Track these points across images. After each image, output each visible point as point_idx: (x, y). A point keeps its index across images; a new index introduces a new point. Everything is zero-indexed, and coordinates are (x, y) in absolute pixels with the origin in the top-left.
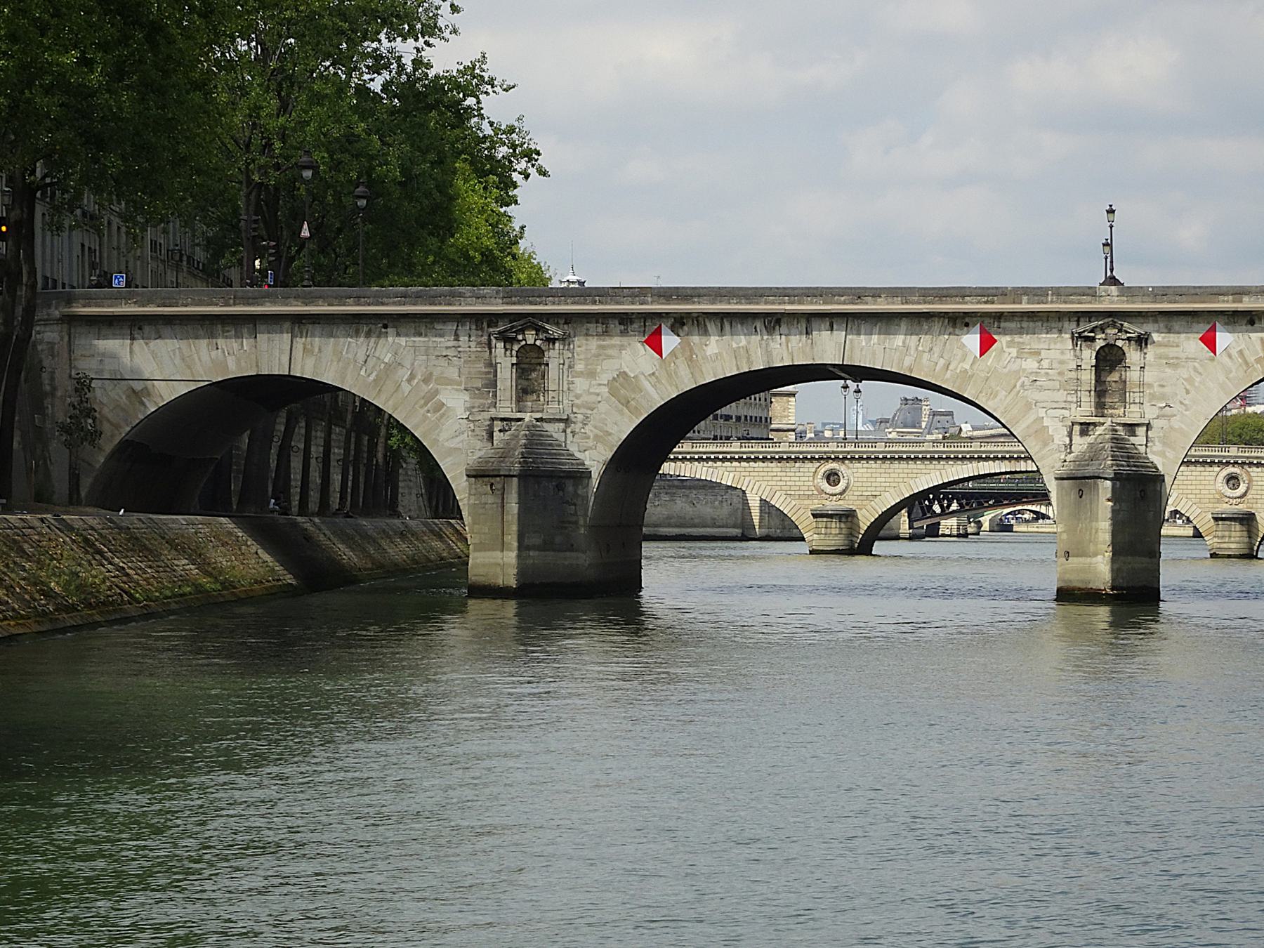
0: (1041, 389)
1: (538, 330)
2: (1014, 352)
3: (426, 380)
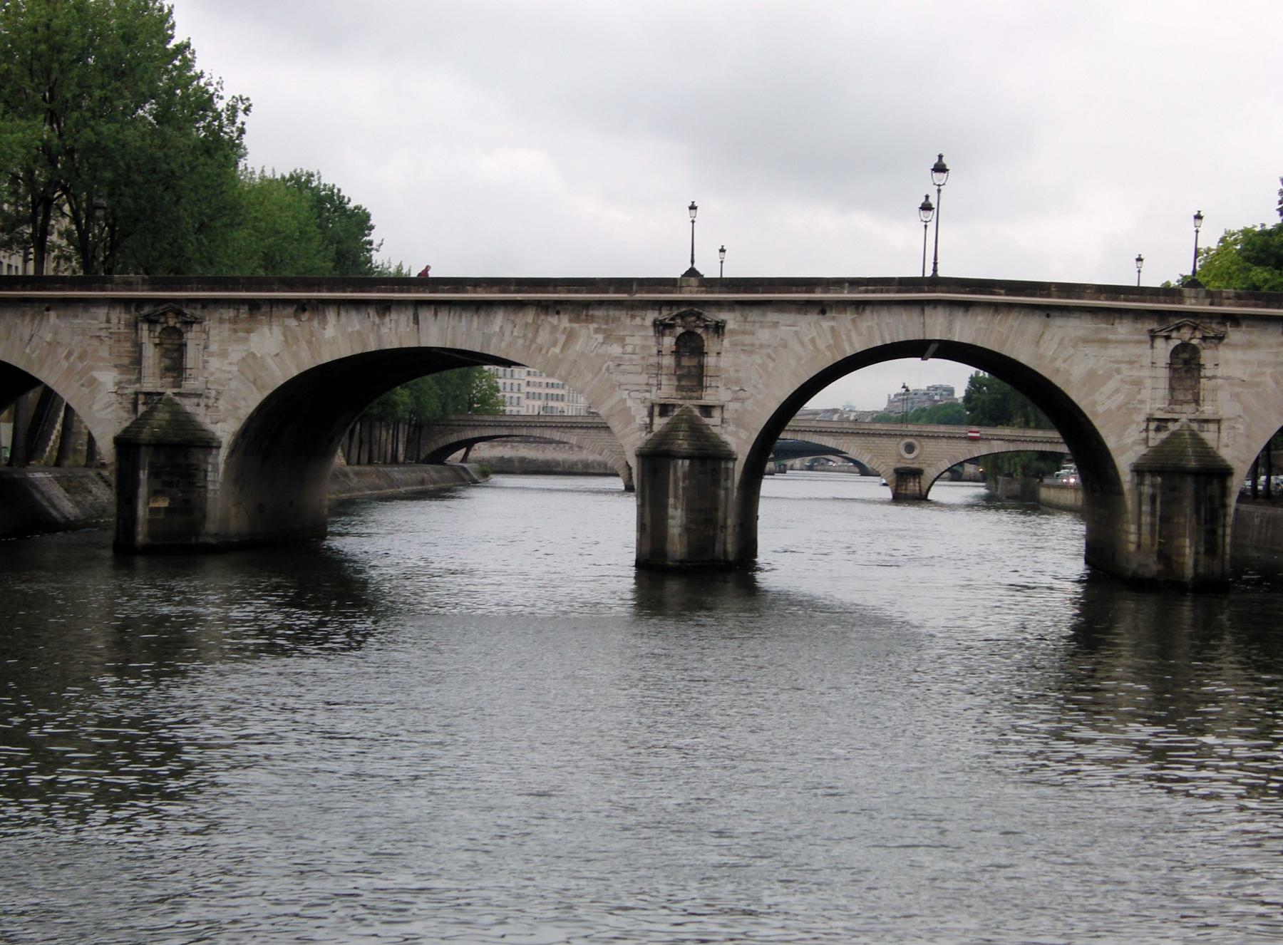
0: (624, 373)
1: (179, 313)
2: (600, 337)
3: (82, 357)
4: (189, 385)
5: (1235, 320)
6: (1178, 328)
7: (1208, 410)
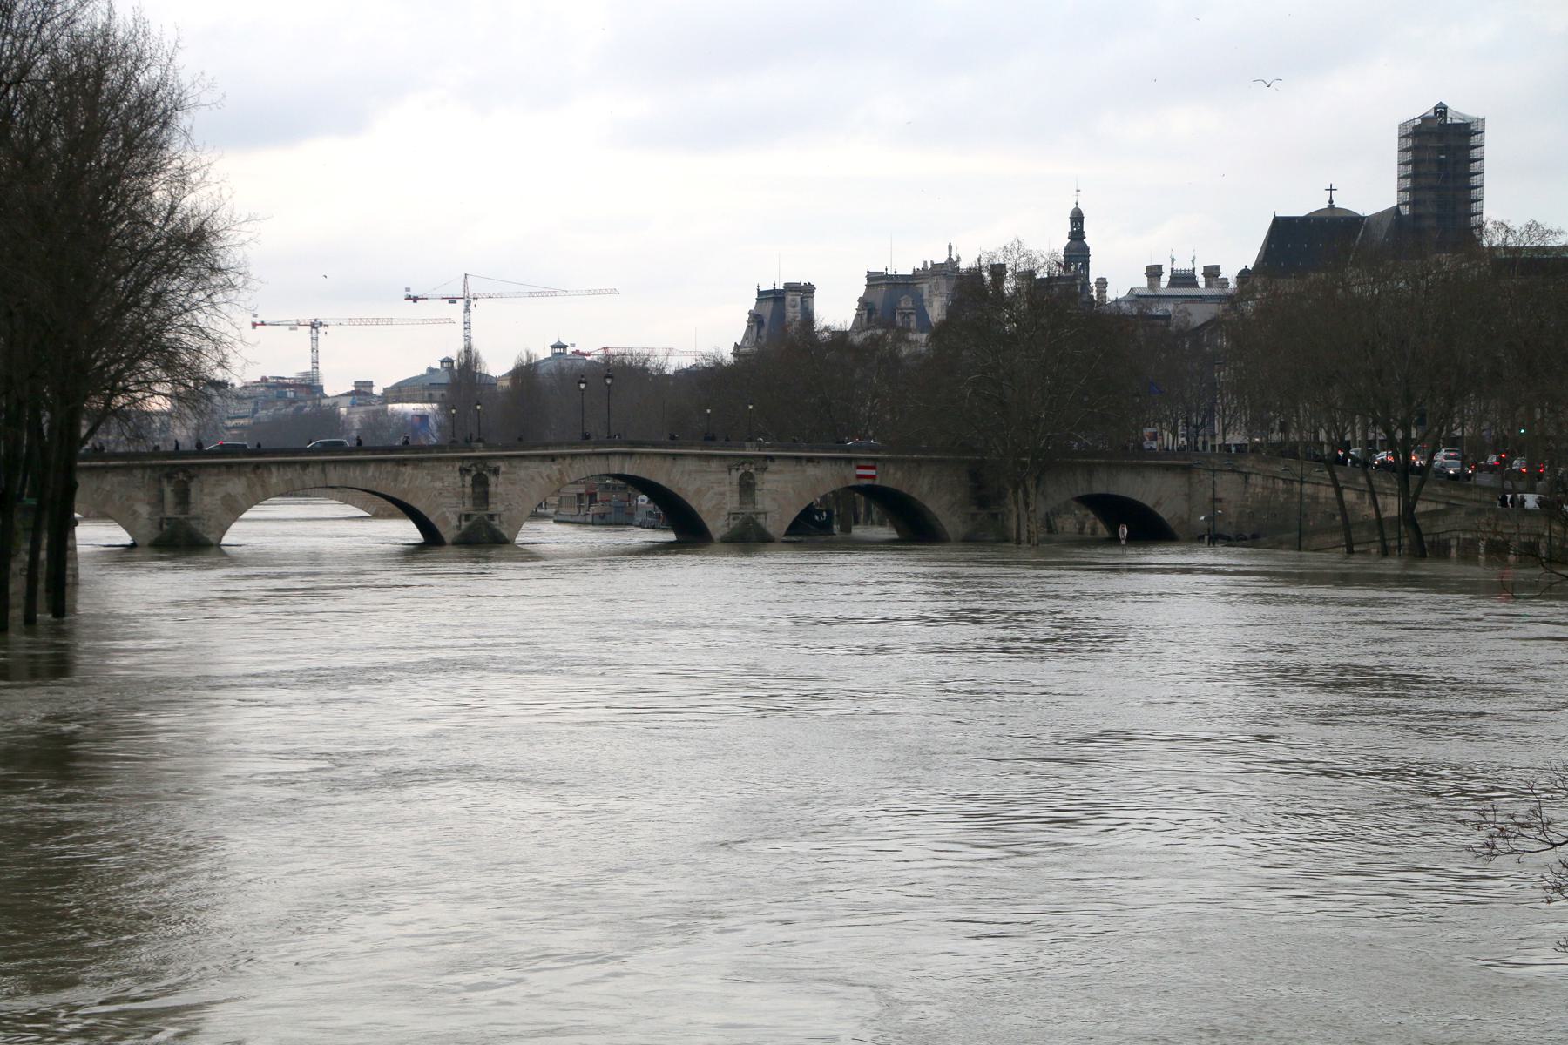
4: (193, 512)
5: (772, 458)
6: (743, 464)
7: (759, 507)
